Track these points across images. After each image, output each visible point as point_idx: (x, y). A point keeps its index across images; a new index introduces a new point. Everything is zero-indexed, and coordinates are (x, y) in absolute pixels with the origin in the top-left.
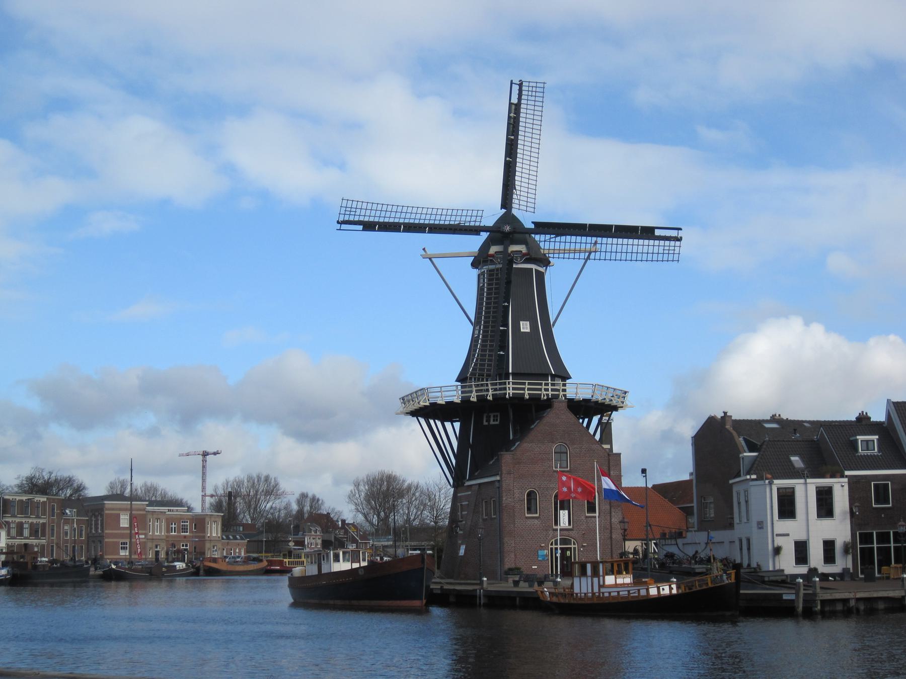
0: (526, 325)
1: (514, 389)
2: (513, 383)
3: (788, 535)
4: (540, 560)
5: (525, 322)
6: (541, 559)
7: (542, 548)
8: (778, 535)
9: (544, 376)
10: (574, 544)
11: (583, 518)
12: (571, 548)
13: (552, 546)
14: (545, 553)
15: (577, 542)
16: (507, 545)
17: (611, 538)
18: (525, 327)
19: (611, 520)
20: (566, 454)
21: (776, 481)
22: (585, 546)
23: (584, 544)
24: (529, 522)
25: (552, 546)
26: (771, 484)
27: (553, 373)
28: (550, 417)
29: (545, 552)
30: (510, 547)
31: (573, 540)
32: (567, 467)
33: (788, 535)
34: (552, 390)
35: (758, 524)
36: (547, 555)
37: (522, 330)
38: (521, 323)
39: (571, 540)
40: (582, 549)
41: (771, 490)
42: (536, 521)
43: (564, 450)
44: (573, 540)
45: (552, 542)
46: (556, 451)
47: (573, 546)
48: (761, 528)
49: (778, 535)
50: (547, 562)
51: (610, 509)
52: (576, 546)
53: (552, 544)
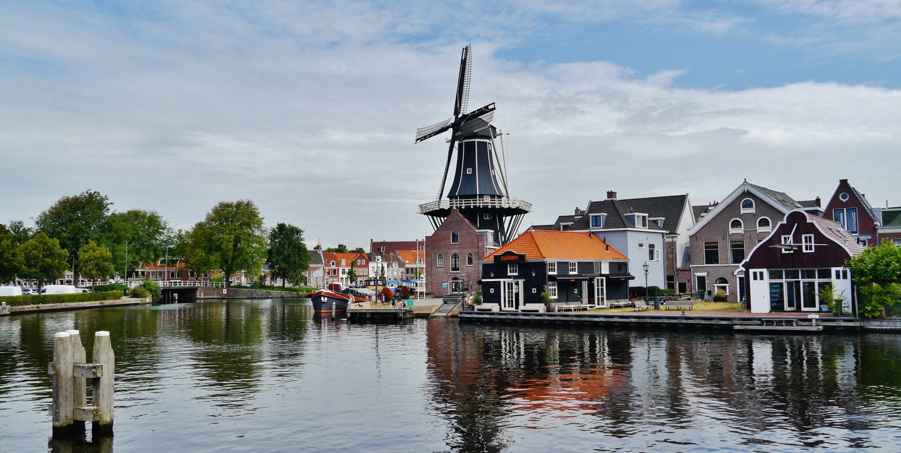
1: (465, 203)
2: (460, 201)
9: (474, 196)
18: (469, 171)
24: (439, 269)
27: (478, 193)
29: (446, 284)
34: (482, 203)
37: (468, 173)
38: (468, 169)
42: (442, 269)
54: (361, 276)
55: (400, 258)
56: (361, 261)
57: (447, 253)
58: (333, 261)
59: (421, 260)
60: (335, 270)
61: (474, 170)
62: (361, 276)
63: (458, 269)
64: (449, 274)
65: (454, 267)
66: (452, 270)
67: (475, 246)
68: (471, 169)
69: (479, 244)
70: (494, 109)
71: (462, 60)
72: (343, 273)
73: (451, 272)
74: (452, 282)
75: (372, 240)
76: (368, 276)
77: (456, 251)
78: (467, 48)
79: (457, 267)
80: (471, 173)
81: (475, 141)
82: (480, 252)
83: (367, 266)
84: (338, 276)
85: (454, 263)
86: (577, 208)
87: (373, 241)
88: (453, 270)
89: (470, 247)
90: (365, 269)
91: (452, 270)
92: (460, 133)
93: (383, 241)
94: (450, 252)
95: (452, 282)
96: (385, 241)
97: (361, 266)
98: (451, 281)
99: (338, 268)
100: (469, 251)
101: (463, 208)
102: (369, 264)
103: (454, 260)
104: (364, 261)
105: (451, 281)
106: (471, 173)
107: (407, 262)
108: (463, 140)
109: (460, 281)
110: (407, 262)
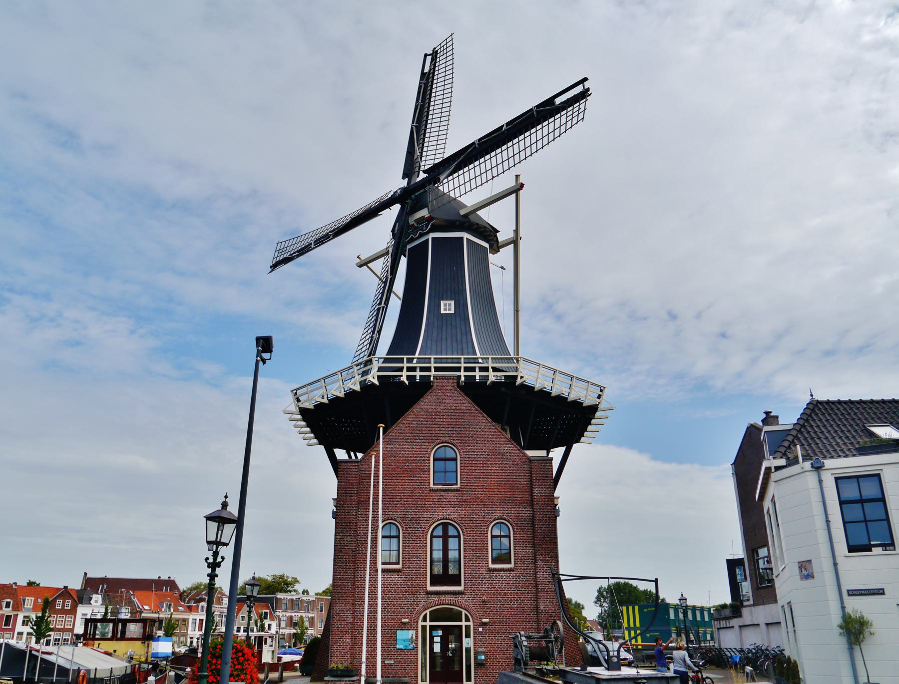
0: (450, 305)
3: (880, 592)
4: (399, 649)
5: (448, 302)
6: (401, 647)
7: (404, 626)
8: (852, 593)
10: (467, 620)
11: (484, 571)
12: (461, 626)
13: (424, 624)
14: (410, 637)
15: (472, 617)
16: (339, 620)
17: (537, 608)
18: (447, 307)
19: (536, 573)
20: (455, 462)
21: (829, 463)
22: (485, 624)
23: (484, 620)
25: (424, 624)
26: (818, 468)
28: (426, 404)
29: (410, 633)
30: (344, 623)
31: (464, 612)
32: (457, 484)
33: (880, 592)
35: (800, 568)
36: (411, 640)
37: (442, 312)
38: (442, 303)
39: (462, 612)
40: (480, 629)
41: (820, 481)
42: (395, 575)
43: (450, 453)
44: (464, 612)
45: (426, 615)
46: (437, 456)
47: (464, 623)
48: (809, 576)
49: (852, 593)
50: (414, 652)
51: (535, 556)
52: (471, 623)
53: (425, 620)
54: (59, 630)
55: (135, 600)
56: (64, 603)
57: (417, 520)
58: (9, 600)
59: (170, 605)
60: (8, 617)
61: (461, 306)
62: (59, 630)
63: (456, 580)
64: (422, 597)
65: (439, 569)
66: (432, 584)
67: (519, 496)
68: (452, 303)
69: (536, 491)
70: (584, 94)
71: (423, 74)
72: (25, 623)
73: (430, 588)
74: (430, 626)
75: (86, 574)
76: (72, 630)
77: (448, 513)
78: (434, 54)
79: (452, 570)
80: (452, 312)
81: (462, 238)
82: (537, 517)
83: (73, 611)
84: (13, 630)
85: (438, 555)
86: (767, 413)
87: (88, 576)
88: (436, 580)
89: (503, 501)
90: (69, 618)
91: (433, 583)
92: (424, 213)
93: (104, 576)
94: (425, 515)
95: (433, 628)
96: (108, 577)
97: (63, 611)
98: (428, 623)
99: (15, 613)
100: (498, 514)
101: (463, 379)
102: (78, 608)
103: (438, 543)
104: (69, 602)
105: (428, 623)
106: (452, 312)
107: (146, 607)
108: (432, 230)
109: (464, 623)
110: (146, 607)
